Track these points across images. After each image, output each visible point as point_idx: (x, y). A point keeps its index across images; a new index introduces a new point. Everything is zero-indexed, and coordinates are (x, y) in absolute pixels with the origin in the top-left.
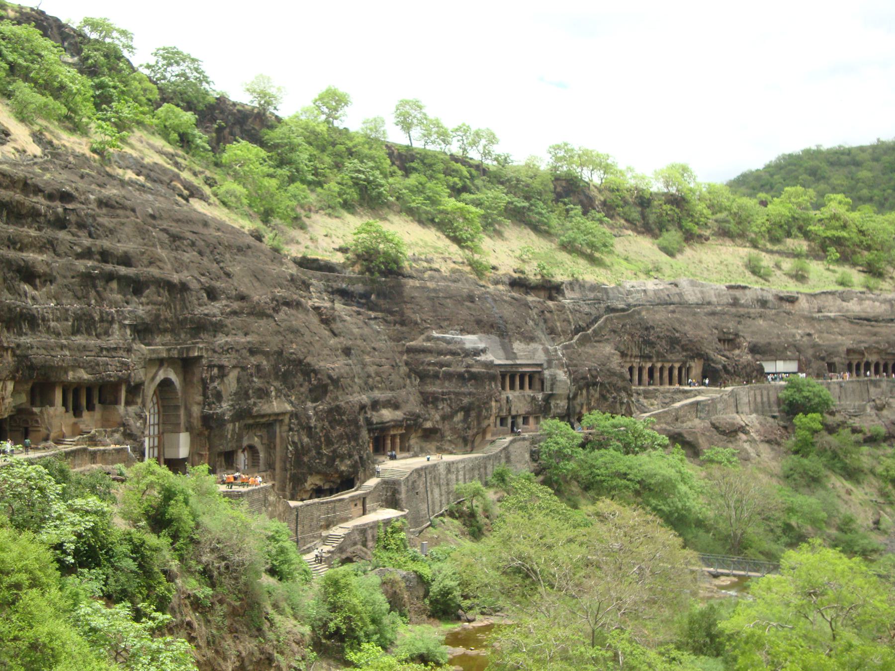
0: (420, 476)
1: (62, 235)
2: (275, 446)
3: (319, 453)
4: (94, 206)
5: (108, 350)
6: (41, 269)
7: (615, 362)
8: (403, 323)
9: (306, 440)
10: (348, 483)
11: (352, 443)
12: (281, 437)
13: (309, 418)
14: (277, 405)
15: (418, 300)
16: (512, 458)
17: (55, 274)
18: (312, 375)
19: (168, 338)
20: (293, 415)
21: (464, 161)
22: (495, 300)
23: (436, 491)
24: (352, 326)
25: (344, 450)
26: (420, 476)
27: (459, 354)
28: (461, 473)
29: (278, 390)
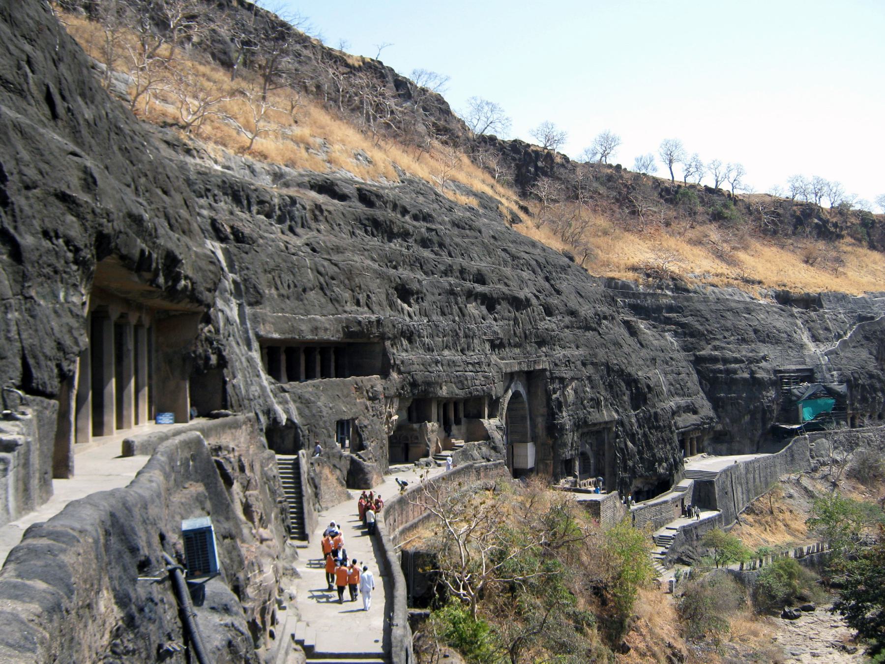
0: (727, 476)
1: (426, 253)
2: (604, 455)
3: (641, 458)
4: (449, 226)
5: (473, 364)
6: (415, 286)
7: (872, 366)
8: (692, 335)
9: (630, 444)
10: (664, 485)
11: (668, 447)
12: (609, 443)
13: (632, 425)
14: (608, 415)
15: (704, 313)
16: (796, 456)
17: (425, 291)
18: (633, 384)
19: (517, 351)
20: (621, 423)
21: (716, 191)
22: (768, 312)
23: (739, 489)
24: (651, 338)
25: (660, 454)
26: (727, 476)
27: (742, 362)
28: (757, 472)
29: (606, 400)
